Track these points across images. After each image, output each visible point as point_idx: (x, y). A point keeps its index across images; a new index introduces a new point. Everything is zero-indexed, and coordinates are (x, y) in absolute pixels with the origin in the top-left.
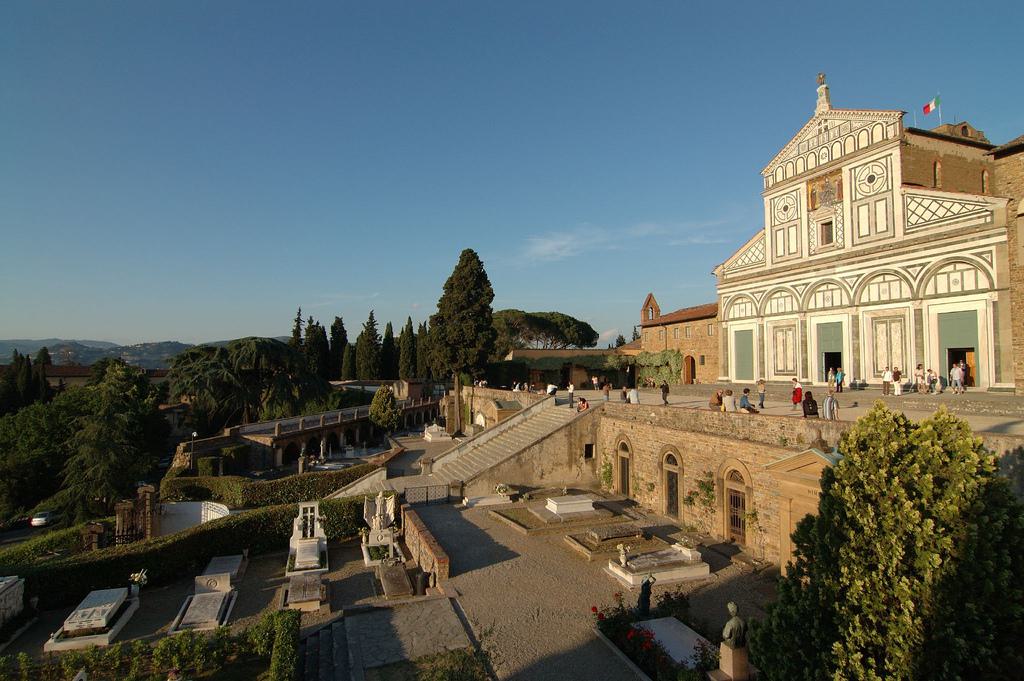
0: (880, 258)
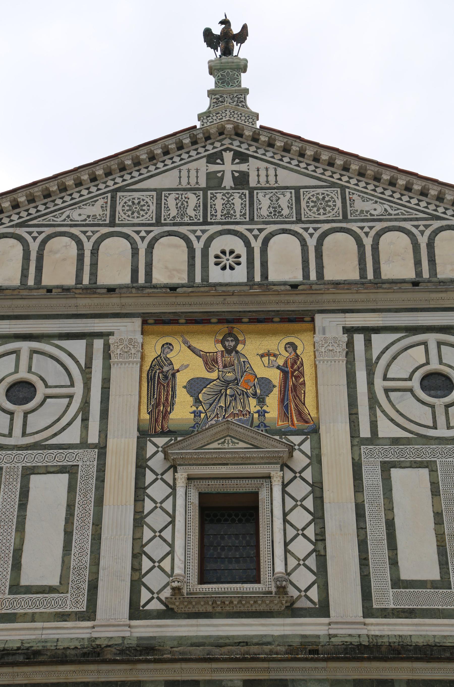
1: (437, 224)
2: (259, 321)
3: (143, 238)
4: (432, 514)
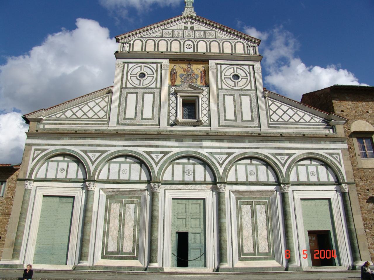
1: (236, 41)
2: (196, 61)
3: (169, 41)
4: (233, 106)
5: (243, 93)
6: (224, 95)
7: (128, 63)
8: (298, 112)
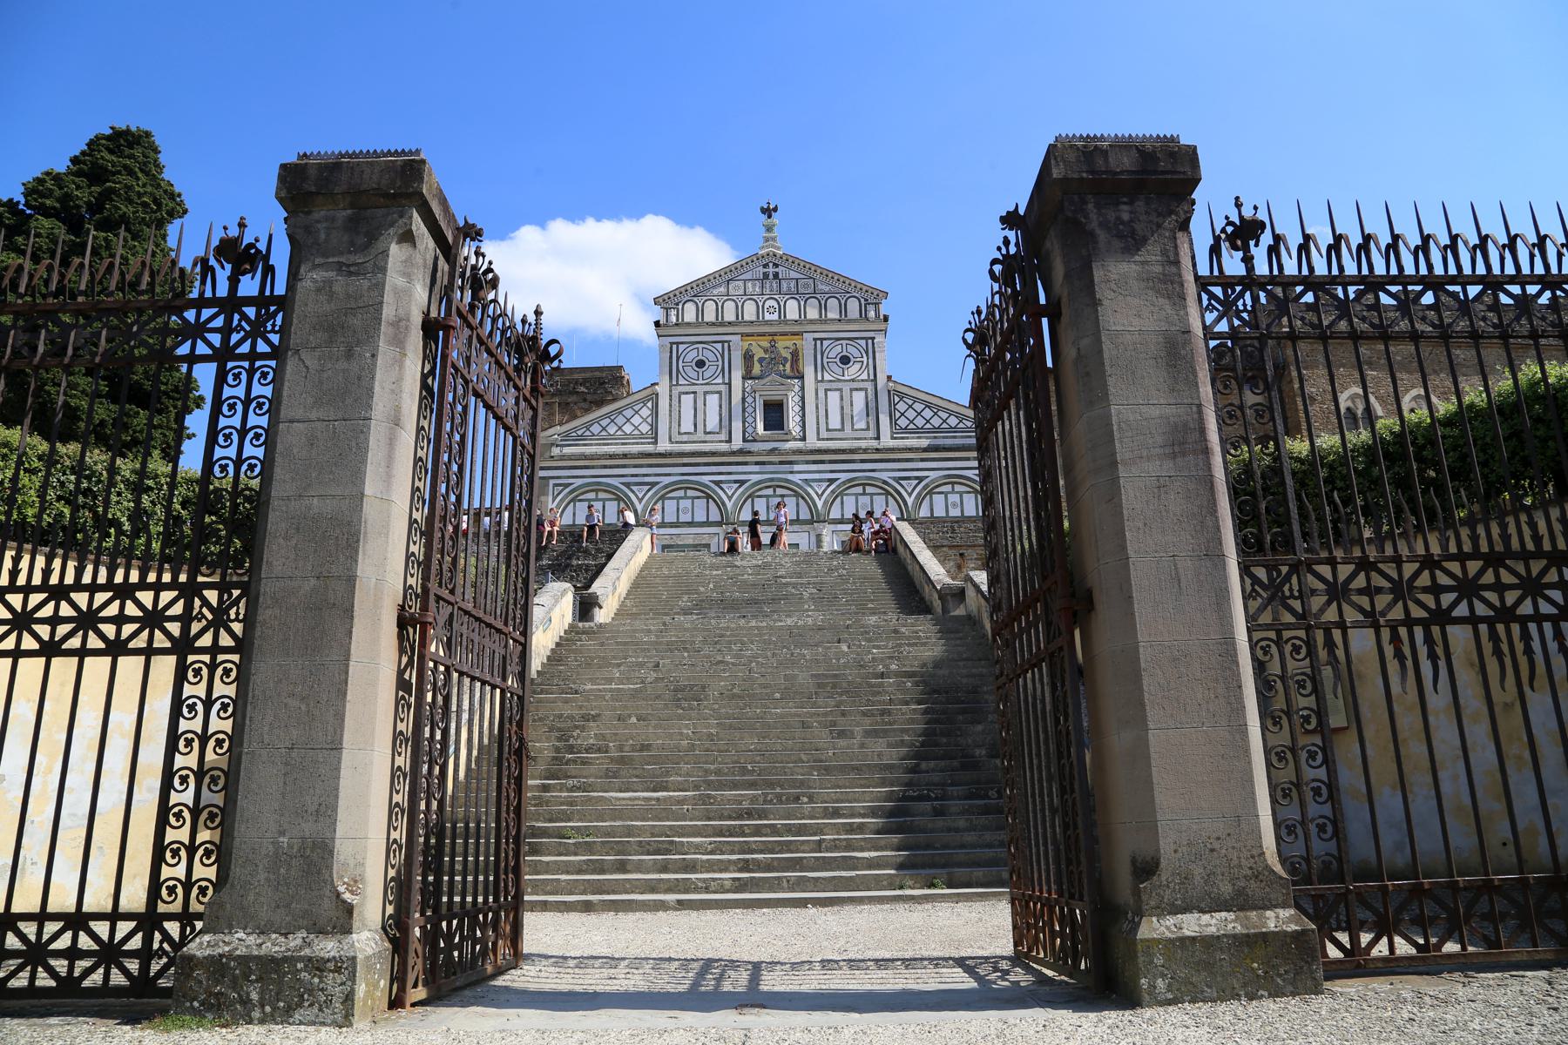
0: (863, 461)
5: (855, 385)
6: (826, 390)
7: (678, 344)
8: (940, 413)
